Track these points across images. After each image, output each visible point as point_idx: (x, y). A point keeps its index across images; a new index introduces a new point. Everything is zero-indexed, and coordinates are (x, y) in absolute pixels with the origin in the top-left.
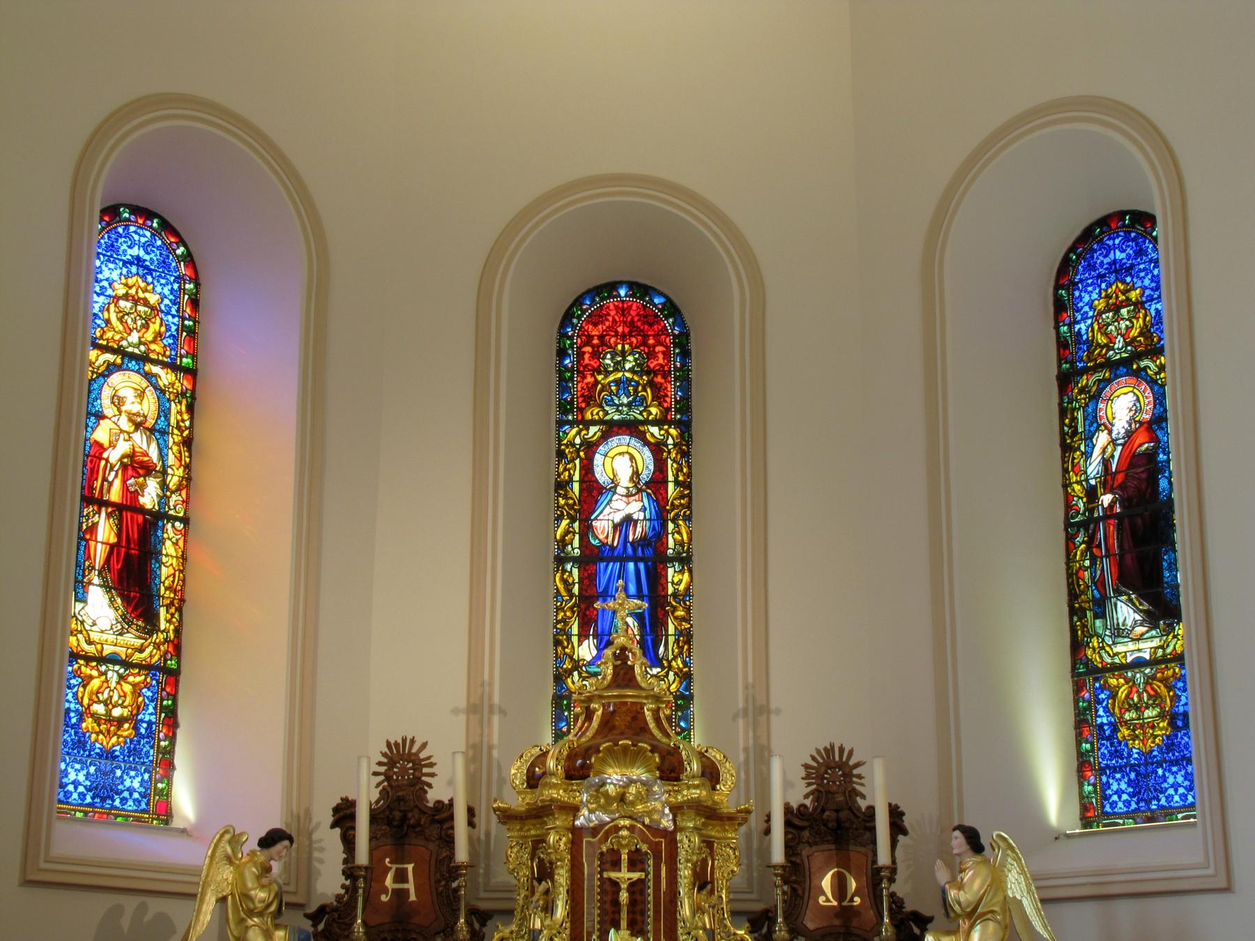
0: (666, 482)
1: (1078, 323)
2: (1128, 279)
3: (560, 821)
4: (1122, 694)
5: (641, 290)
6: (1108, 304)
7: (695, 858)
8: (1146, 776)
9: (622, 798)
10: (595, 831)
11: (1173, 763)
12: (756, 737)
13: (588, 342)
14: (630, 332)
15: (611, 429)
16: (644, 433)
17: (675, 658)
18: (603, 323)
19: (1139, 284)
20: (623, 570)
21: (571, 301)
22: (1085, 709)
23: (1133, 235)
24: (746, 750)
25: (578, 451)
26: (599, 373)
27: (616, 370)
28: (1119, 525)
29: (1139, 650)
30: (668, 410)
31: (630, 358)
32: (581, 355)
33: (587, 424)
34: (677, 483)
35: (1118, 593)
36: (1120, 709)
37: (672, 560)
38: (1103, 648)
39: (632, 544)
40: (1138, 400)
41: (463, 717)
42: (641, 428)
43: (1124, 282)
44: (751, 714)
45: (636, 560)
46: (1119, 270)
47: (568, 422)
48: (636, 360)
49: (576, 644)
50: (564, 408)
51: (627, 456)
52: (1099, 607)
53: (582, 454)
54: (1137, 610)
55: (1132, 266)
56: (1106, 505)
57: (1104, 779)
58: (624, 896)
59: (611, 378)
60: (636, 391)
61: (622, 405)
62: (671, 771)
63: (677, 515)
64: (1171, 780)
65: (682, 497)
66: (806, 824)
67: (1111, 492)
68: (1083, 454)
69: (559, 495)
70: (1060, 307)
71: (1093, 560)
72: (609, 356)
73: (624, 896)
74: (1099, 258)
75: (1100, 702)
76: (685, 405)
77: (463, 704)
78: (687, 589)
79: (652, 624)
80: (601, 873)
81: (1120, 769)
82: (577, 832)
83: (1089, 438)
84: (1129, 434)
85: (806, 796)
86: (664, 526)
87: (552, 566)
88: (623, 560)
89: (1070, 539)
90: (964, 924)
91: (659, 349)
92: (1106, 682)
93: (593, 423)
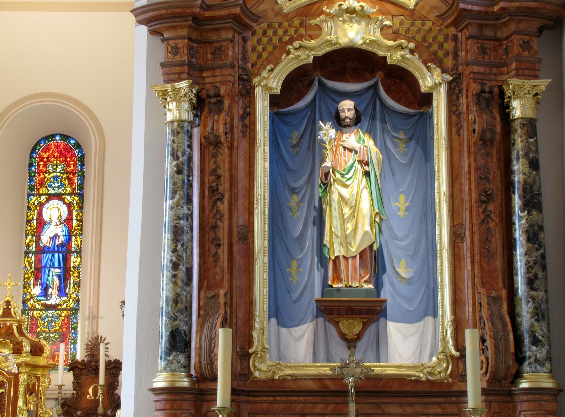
0: (72, 220)
5: (65, 137)
7: (25, 384)
12: (92, 328)
13: (42, 160)
14: (60, 156)
15: (51, 197)
16: (64, 199)
17: (73, 293)
18: (48, 152)
20: (53, 257)
21: (35, 143)
24: (88, 333)
25: (36, 207)
26: (46, 173)
27: (53, 172)
30: (74, 189)
31: (60, 167)
32: (39, 166)
33: (40, 195)
34: (77, 220)
37: (73, 252)
39: (57, 246)
42: (63, 197)
44: (91, 318)
45: (59, 252)
47: (32, 195)
48: (62, 168)
49: (32, 288)
50: (31, 188)
51: (57, 209)
53: (38, 208)
59: (51, 175)
60: (61, 181)
61: (55, 187)
63: (76, 233)
65: (79, 226)
66: (83, 367)
69: (28, 225)
72: (51, 166)
76: (81, 187)
78: (79, 264)
79: (64, 279)
85: (86, 356)
86: (71, 238)
87: (23, 255)
88: (53, 252)
91: (72, 163)
93: (43, 195)
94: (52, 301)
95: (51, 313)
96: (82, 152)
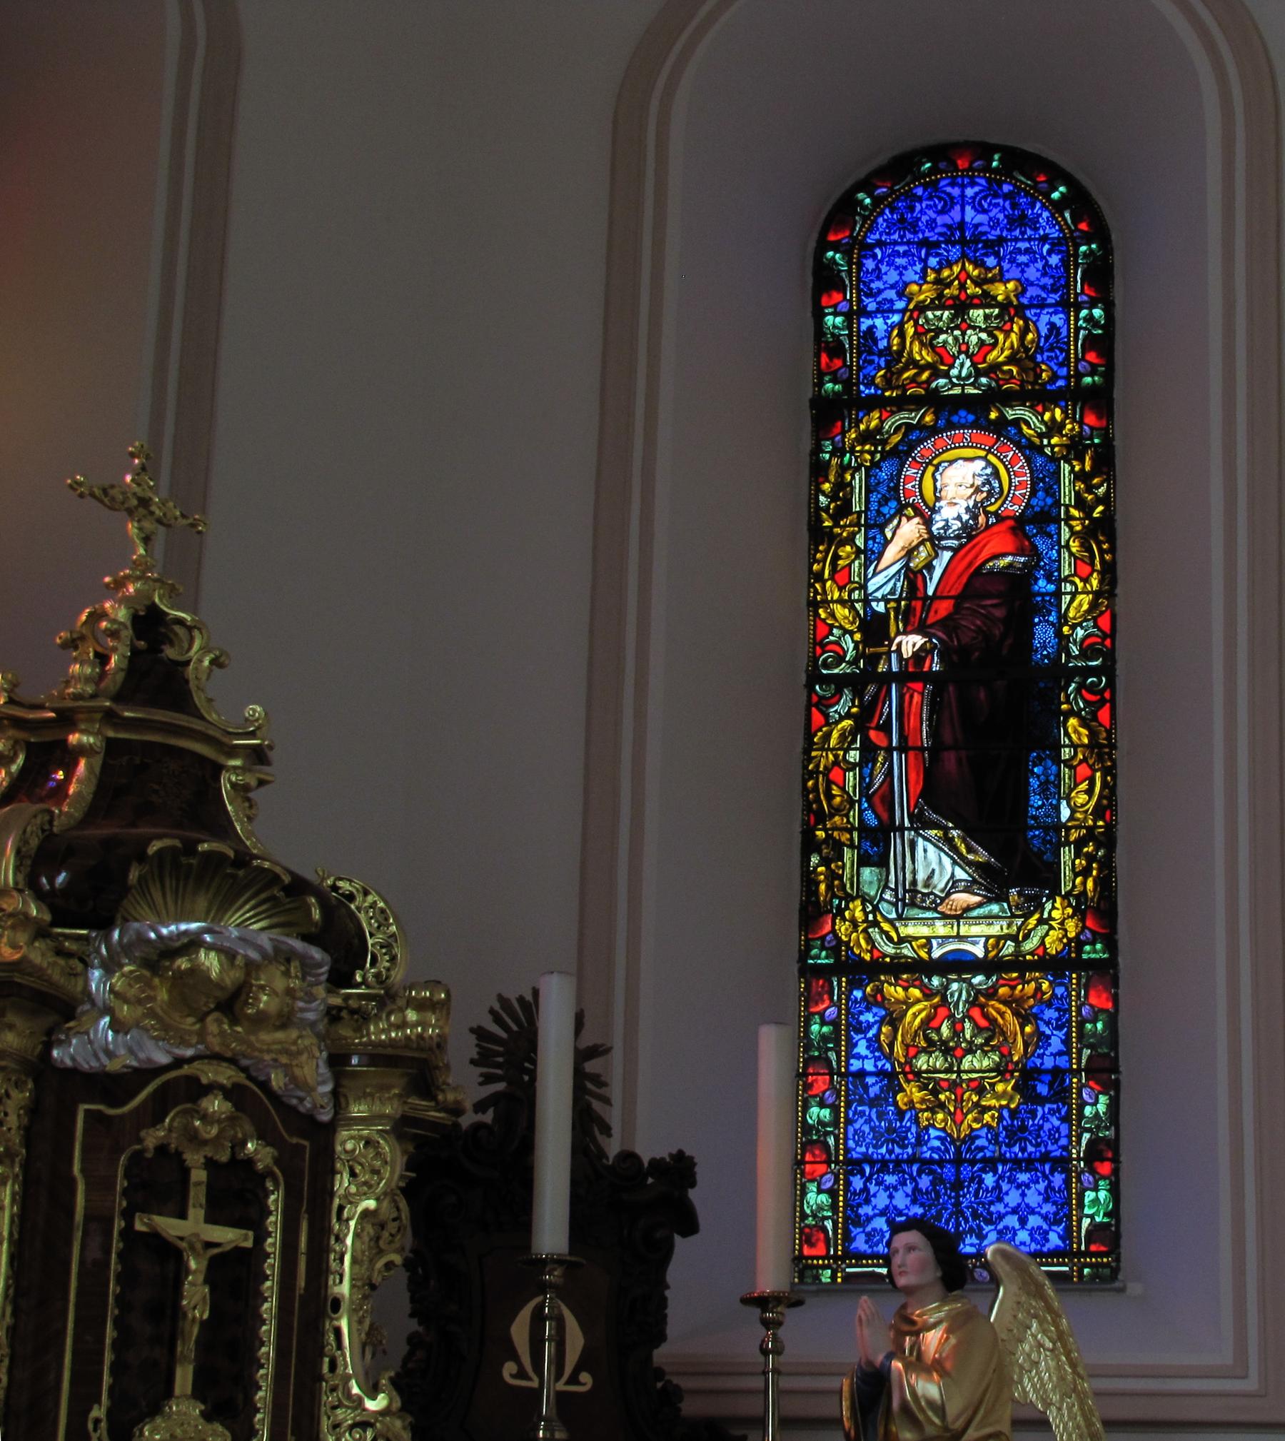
1: (870, 315)
2: (991, 261)
4: (915, 1016)
6: (940, 296)
8: (958, 1185)
10: (111, 1086)
11: (1017, 1164)
19: (1015, 272)
22: (824, 1038)
23: (1006, 188)
28: (933, 695)
29: (959, 937)
35: (920, 823)
36: (907, 1047)
38: (875, 924)
40: (996, 473)
43: (978, 263)
46: (972, 244)
52: (875, 843)
54: (960, 860)
55: (1001, 241)
56: (907, 652)
57: (858, 1183)
58: (196, 1298)
64: (1013, 1198)
67: (920, 630)
68: (858, 552)
71: (869, 752)
73: (196, 1298)
74: (925, 212)
75: (861, 1029)
80: (128, 1215)
81: (898, 1165)
83: (877, 526)
84: (969, 532)
92: (879, 990)
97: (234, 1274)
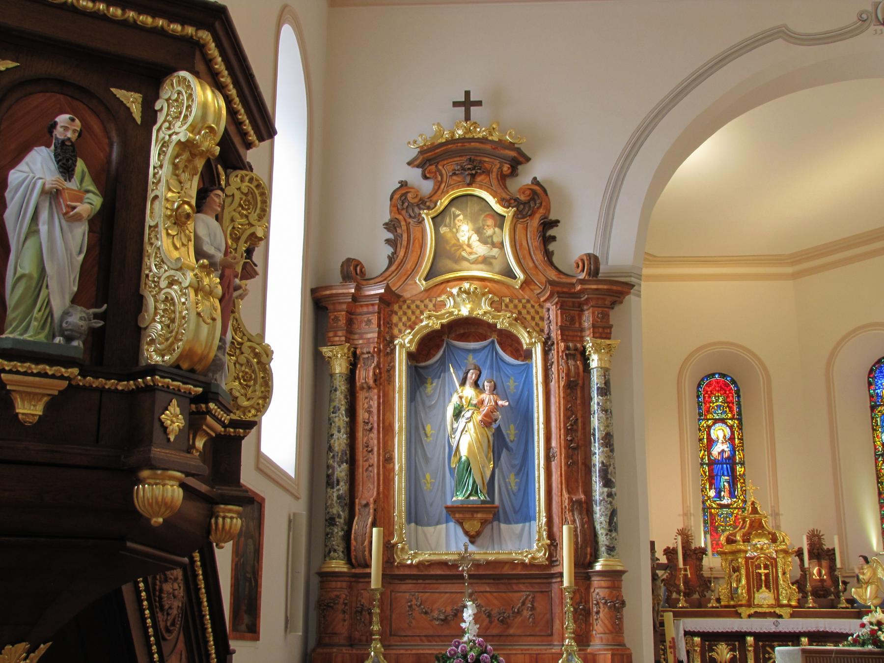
3: (742, 555)
5: (723, 375)
9: (762, 549)
10: (752, 558)
13: (707, 393)
15: (716, 421)
33: (708, 420)
41: (682, 517)
50: (700, 414)
58: (763, 577)
62: (774, 540)
70: (870, 384)
73: (763, 577)
76: (740, 414)
77: (681, 513)
82: (747, 559)
88: (722, 464)
89: (876, 459)
90: (864, 586)
94: (725, 502)
95: (725, 511)
96: (737, 387)
97: (767, 575)
